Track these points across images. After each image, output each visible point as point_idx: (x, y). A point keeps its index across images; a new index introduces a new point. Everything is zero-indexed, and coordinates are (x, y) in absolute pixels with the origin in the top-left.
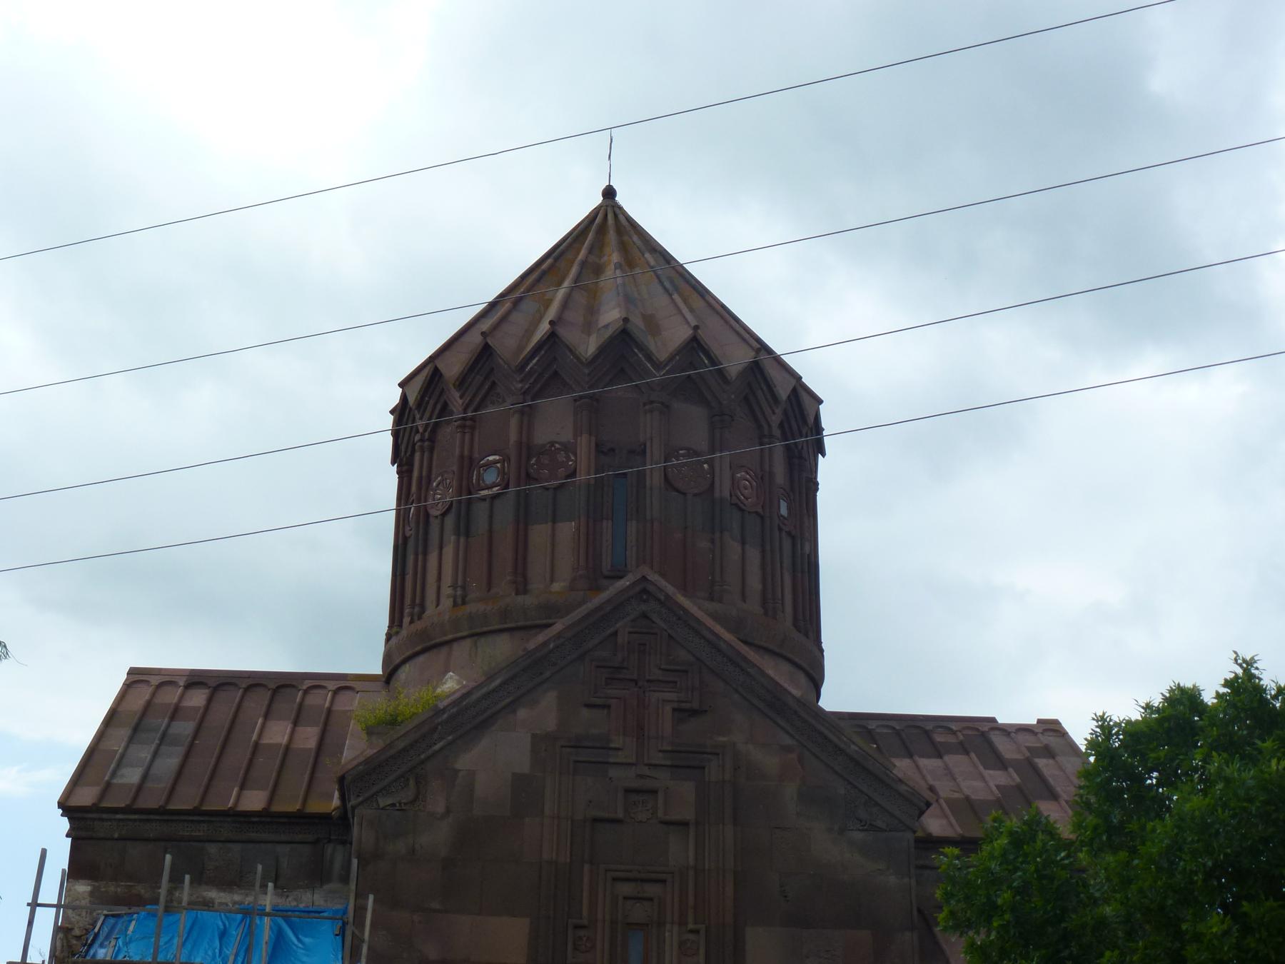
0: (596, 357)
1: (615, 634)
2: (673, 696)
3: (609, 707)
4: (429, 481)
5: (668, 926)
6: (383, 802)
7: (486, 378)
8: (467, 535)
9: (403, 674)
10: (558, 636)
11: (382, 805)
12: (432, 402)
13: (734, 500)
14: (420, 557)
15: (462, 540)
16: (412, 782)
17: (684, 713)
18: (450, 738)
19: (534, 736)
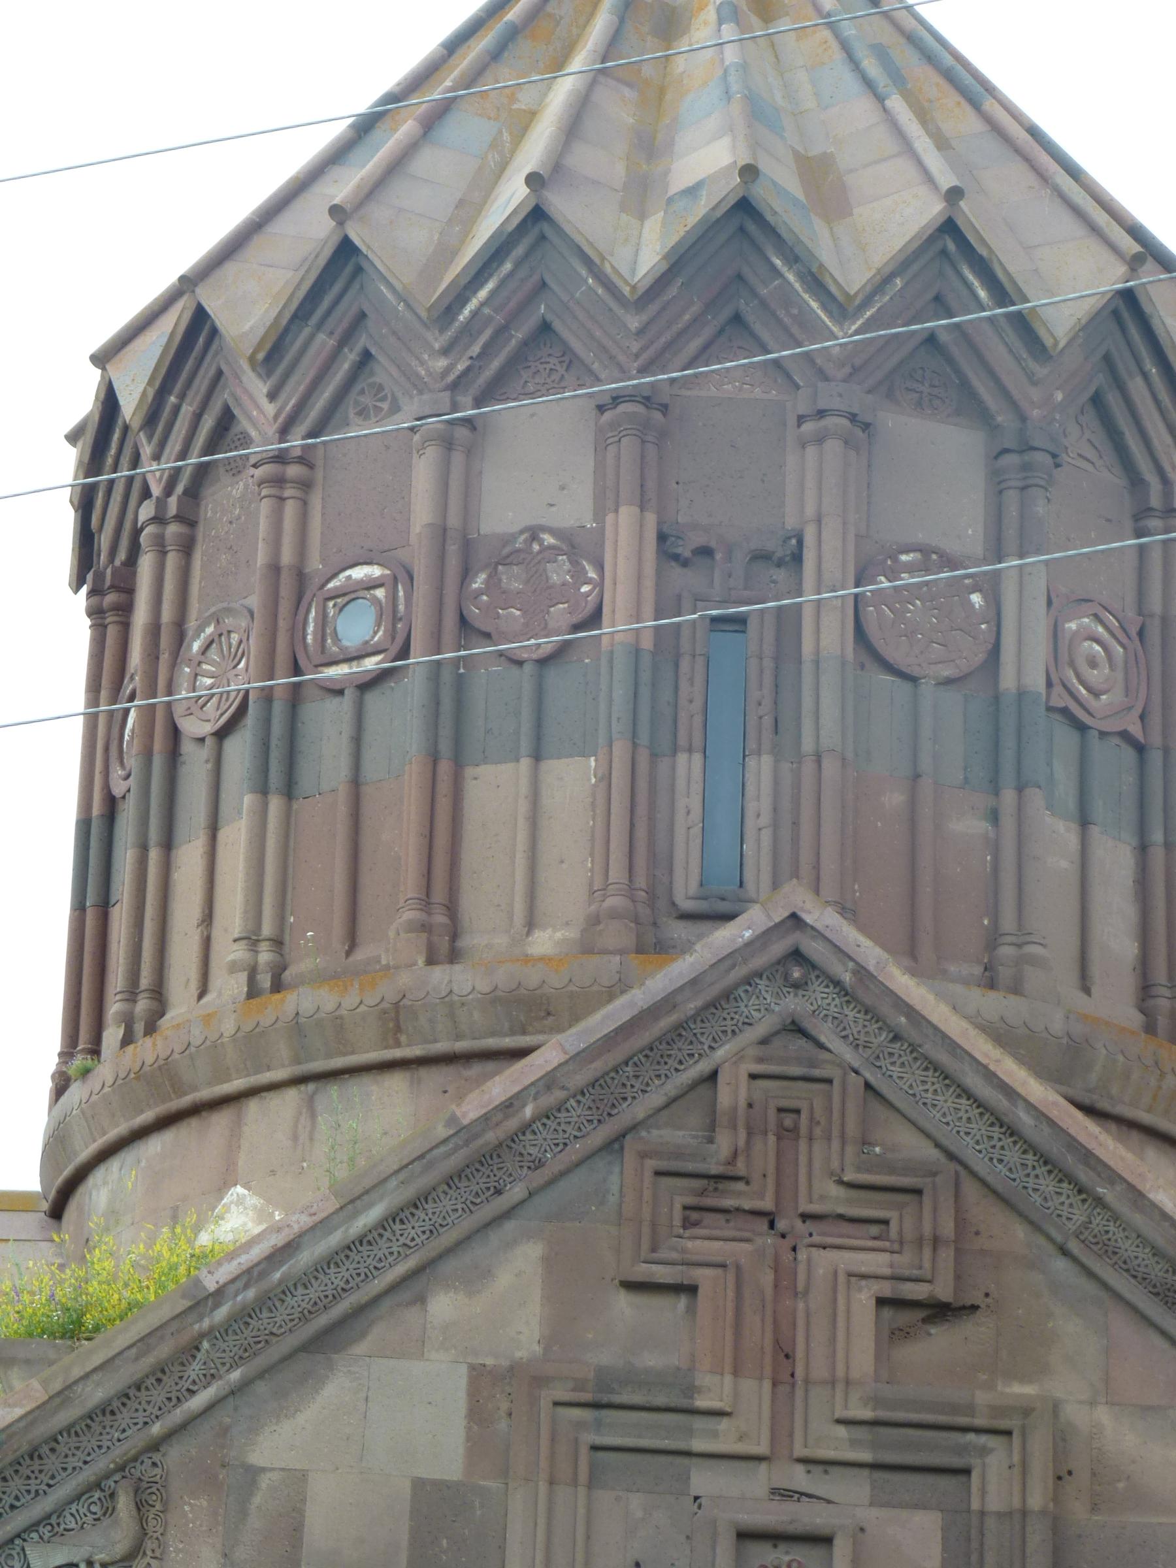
0: (661, 282)
2: (877, 1262)
3: (691, 1290)
4: (180, 637)
7: (346, 340)
8: (289, 791)
9: (99, 1192)
10: (549, 1081)
12: (187, 410)
13: (1060, 699)
14: (154, 855)
15: (275, 804)
16: (124, 1503)
17: (915, 1312)
18: (235, 1375)
19: (479, 1377)
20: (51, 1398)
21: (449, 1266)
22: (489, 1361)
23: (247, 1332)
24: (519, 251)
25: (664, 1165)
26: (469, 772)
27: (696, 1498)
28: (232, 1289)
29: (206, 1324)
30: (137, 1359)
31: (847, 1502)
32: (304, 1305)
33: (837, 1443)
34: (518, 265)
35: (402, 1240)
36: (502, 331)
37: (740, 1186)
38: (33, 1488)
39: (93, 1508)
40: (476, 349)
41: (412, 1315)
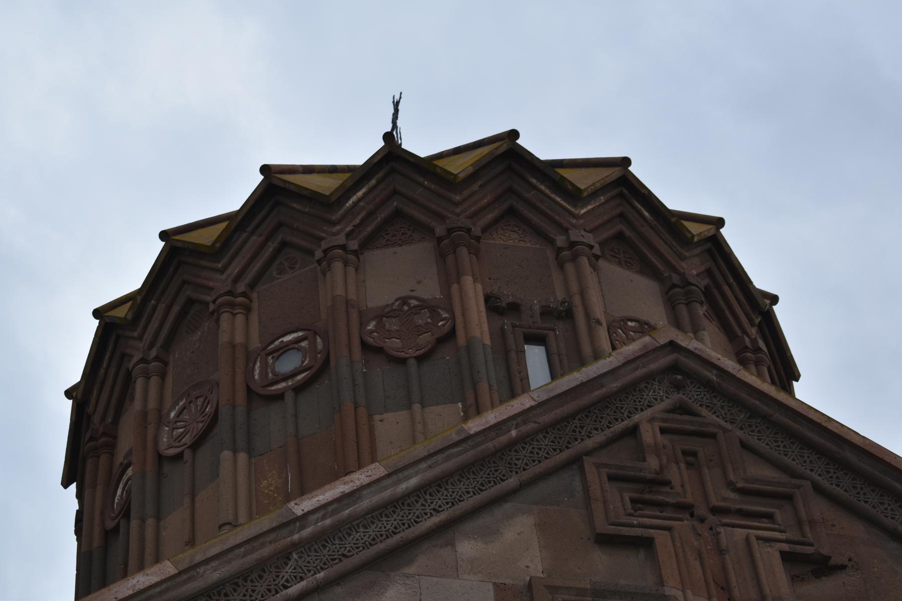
1: (633, 431)
8: (250, 451)
12: (162, 307)
14: (150, 522)
15: (242, 457)
18: (321, 575)
23: (325, 552)
24: (380, 175)
25: (613, 471)
26: (377, 417)
29: (296, 537)
30: (244, 556)
32: (365, 539)
34: (379, 182)
35: (432, 506)
36: (371, 214)
37: (667, 489)
40: (357, 221)
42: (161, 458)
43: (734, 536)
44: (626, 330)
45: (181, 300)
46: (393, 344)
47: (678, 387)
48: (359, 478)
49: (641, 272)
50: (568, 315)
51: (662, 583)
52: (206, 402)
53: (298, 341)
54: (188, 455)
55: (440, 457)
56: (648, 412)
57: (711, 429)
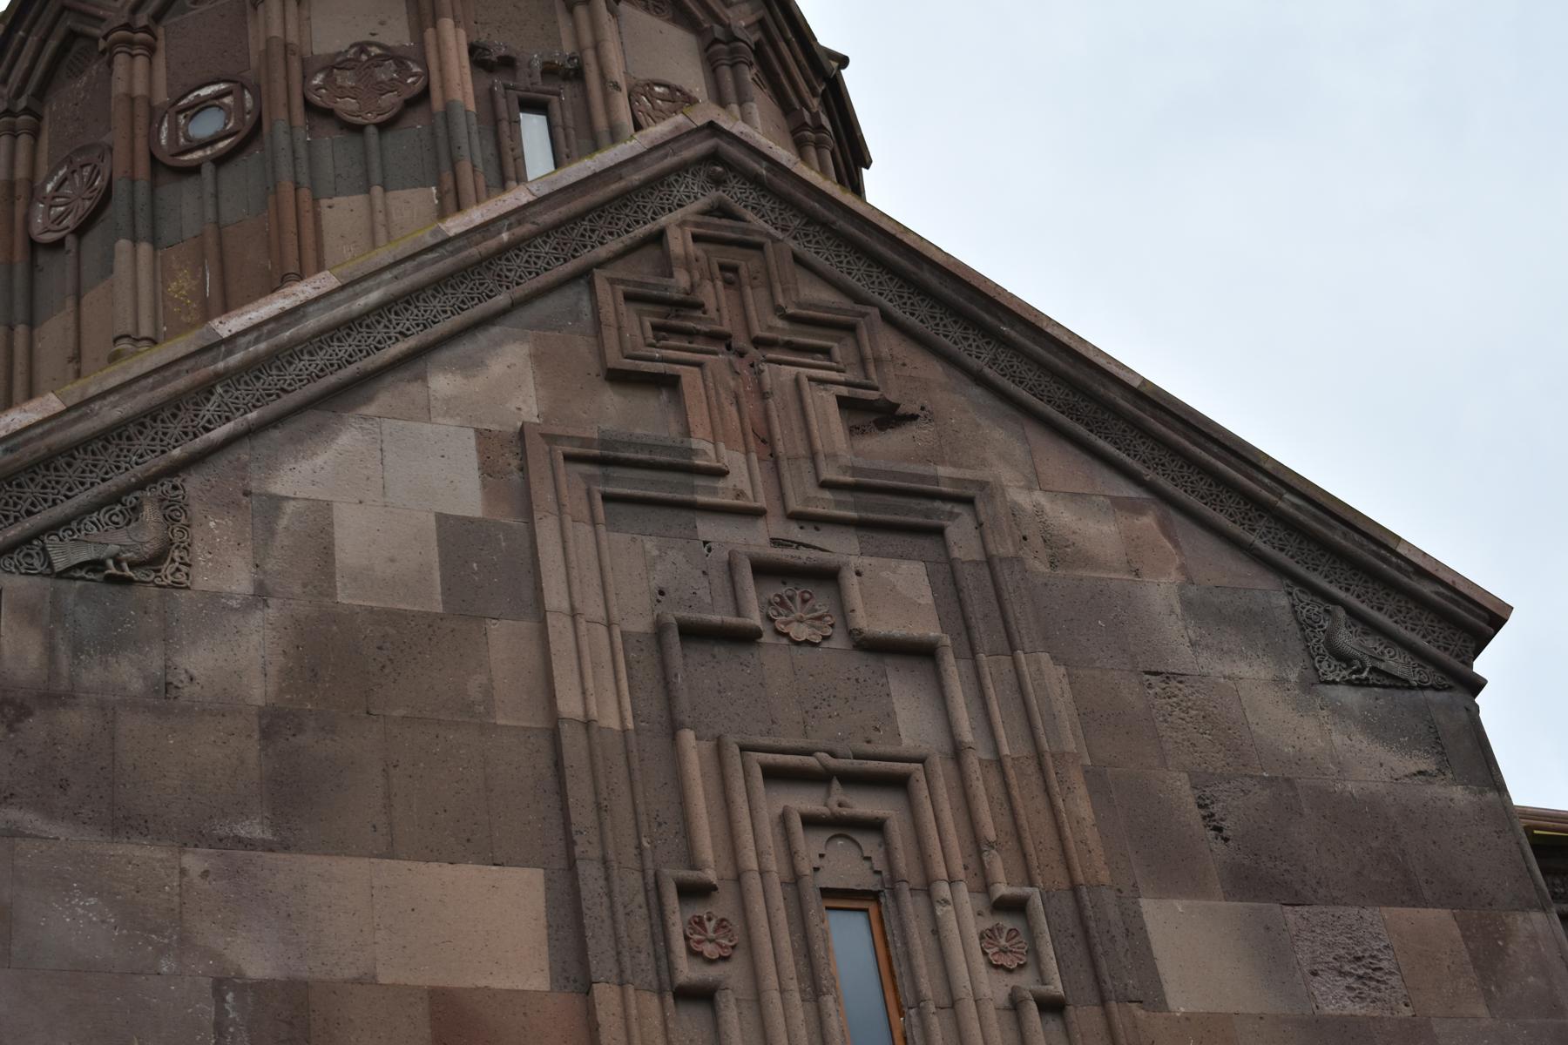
1: (659, 237)
5: (943, 890)
6: (64, 554)
8: (154, 241)
11: (60, 563)
14: (21, 330)
15: (145, 248)
16: (150, 513)
18: (252, 416)
20: (69, 410)
21: (446, 354)
22: (494, 427)
23: (259, 385)
25: (630, 289)
26: (324, 202)
27: (705, 543)
28: (243, 340)
29: (221, 365)
30: (153, 388)
31: (840, 548)
33: (825, 503)
35: (399, 328)
37: (699, 314)
38: (50, 497)
39: (114, 518)
41: (415, 388)
42: (33, 246)
43: (780, 376)
44: (652, 98)
45: (60, 31)
46: (347, 106)
47: (718, 182)
48: (304, 291)
49: (674, 21)
50: (576, 74)
51: (687, 433)
52: (96, 172)
53: (219, 95)
54: (70, 242)
55: (409, 265)
56: (678, 214)
57: (757, 238)
